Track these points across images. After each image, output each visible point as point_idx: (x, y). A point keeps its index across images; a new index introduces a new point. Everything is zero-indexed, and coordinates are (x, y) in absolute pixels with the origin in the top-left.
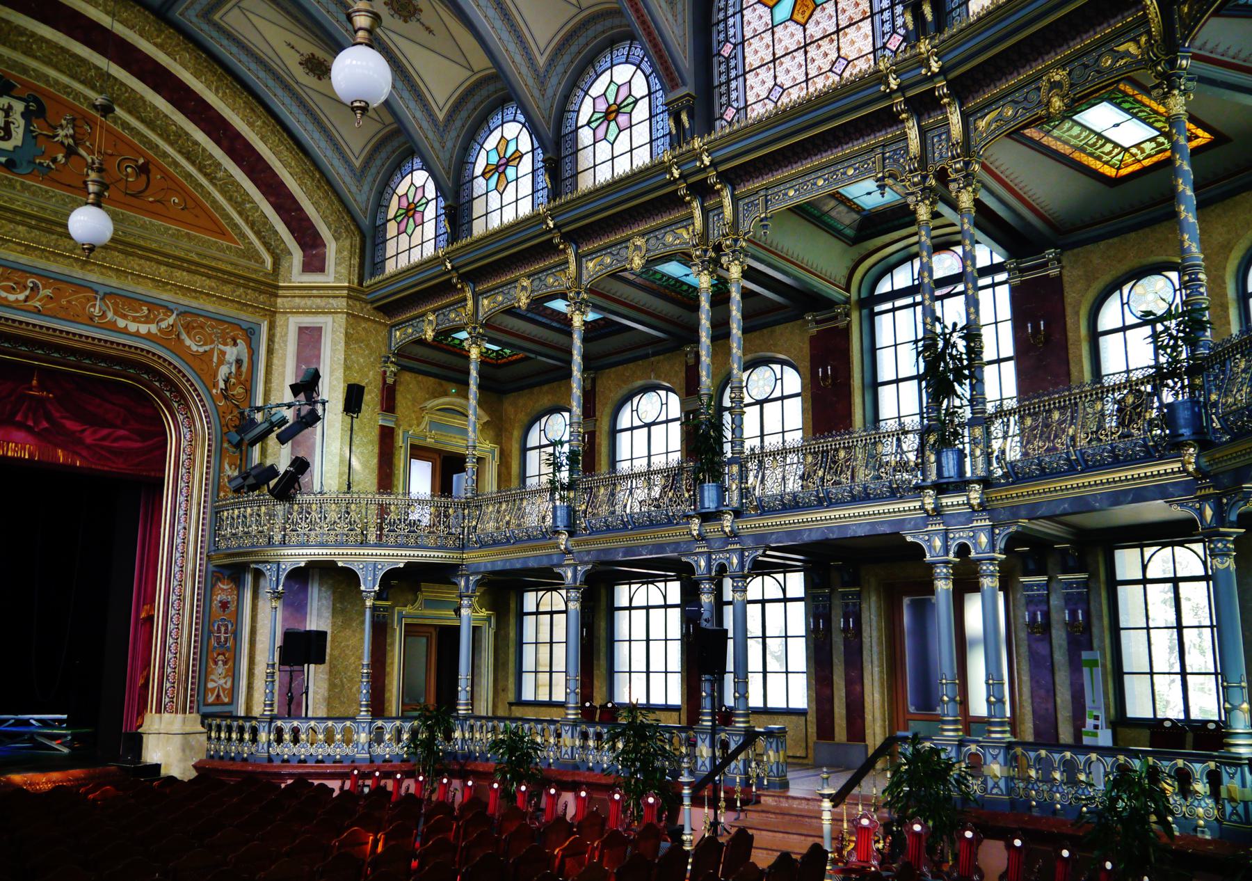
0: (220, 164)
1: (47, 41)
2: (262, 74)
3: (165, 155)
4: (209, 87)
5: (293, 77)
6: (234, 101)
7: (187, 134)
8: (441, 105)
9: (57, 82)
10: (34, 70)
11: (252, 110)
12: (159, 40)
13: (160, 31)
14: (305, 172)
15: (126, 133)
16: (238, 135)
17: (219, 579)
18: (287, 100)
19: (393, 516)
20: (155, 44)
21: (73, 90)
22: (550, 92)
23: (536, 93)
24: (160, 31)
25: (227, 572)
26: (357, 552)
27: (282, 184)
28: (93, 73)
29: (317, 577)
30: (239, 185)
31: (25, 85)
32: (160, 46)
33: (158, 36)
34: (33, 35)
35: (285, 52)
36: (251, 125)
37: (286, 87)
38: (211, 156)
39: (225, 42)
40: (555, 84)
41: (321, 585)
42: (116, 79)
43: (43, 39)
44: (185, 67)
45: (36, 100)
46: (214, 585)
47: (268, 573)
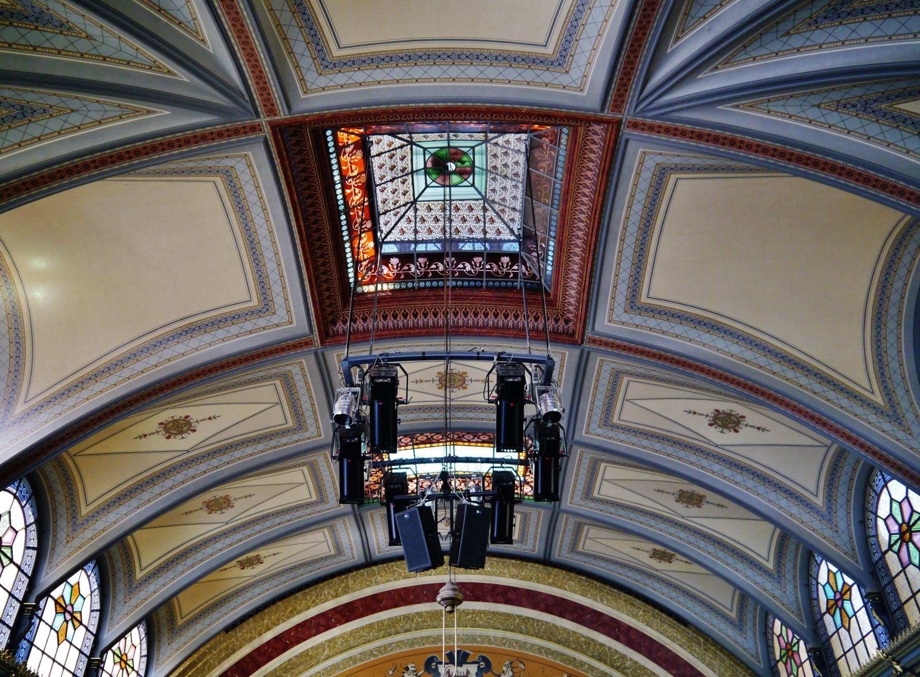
0: (625, 656)
1: (483, 612)
2: (630, 574)
3: (582, 664)
4: (595, 600)
5: (651, 568)
6: (617, 603)
7: (593, 640)
8: (765, 556)
9: (496, 638)
10: (480, 636)
11: (632, 604)
12: (551, 581)
13: (549, 574)
14: (691, 640)
15: (550, 658)
16: (630, 628)
18: (657, 585)
20: (549, 584)
21: (507, 639)
22: (842, 525)
23: (828, 533)
24: (549, 574)
27: (676, 657)
28: (517, 620)
30: (645, 668)
31: (475, 650)
32: (553, 584)
33: (549, 578)
34: (474, 612)
35: (636, 554)
36: (635, 616)
37: (651, 576)
38: (616, 652)
39: (595, 562)
40: (845, 520)
42: (533, 619)
43: (480, 612)
44: (575, 592)
45: (484, 659)
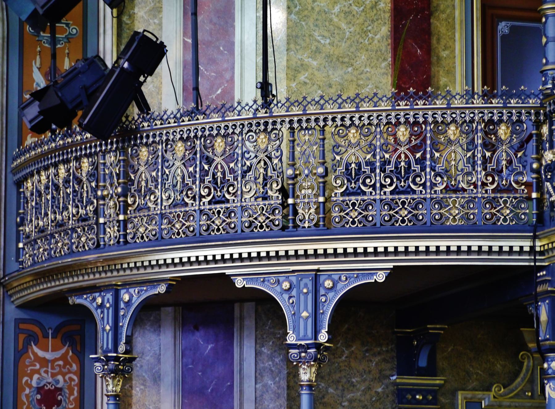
17: (32, 338)
19: (353, 156)
25: (52, 321)
26: (282, 249)
29: (250, 323)
41: (259, 341)
46: (20, 354)
47: (97, 314)
